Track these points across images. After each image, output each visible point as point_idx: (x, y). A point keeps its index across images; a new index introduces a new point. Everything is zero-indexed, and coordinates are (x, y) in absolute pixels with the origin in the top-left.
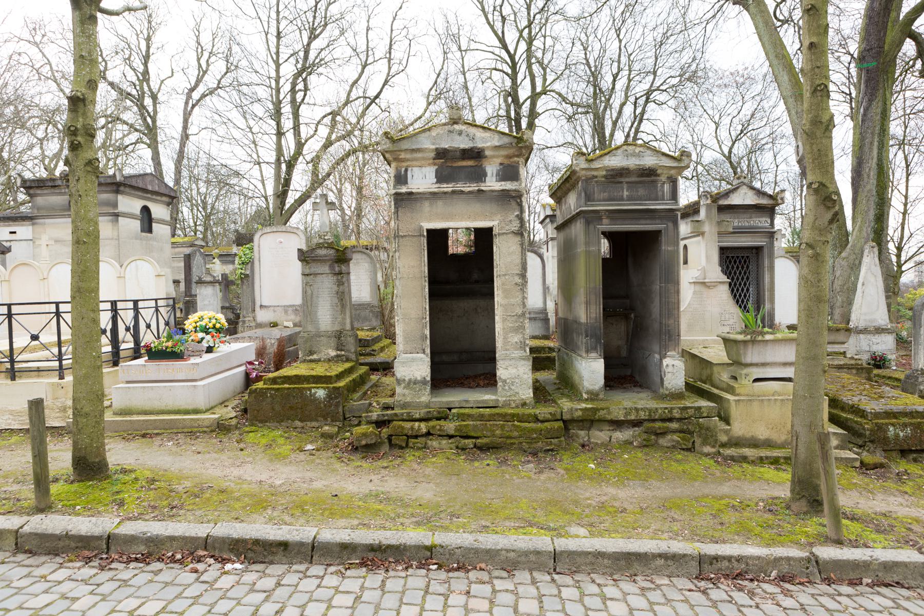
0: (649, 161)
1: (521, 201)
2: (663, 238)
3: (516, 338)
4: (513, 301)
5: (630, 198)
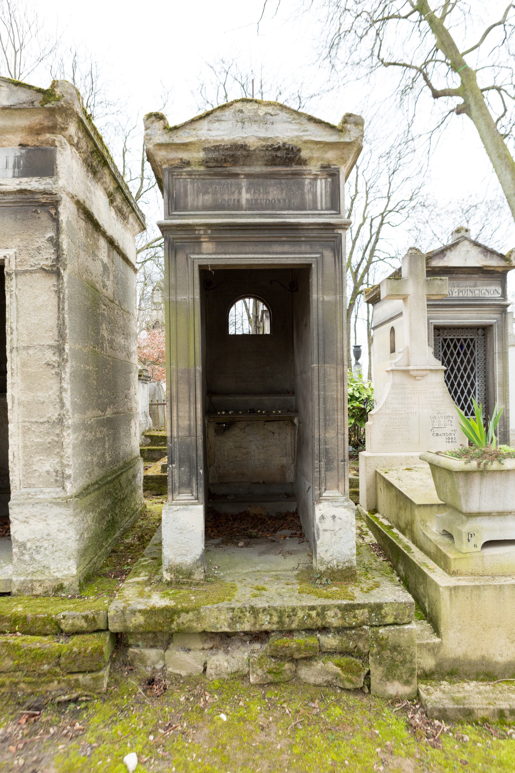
0: (284, 132)
1: (57, 213)
2: (315, 280)
3: (47, 465)
4: (41, 395)
5: (253, 206)
